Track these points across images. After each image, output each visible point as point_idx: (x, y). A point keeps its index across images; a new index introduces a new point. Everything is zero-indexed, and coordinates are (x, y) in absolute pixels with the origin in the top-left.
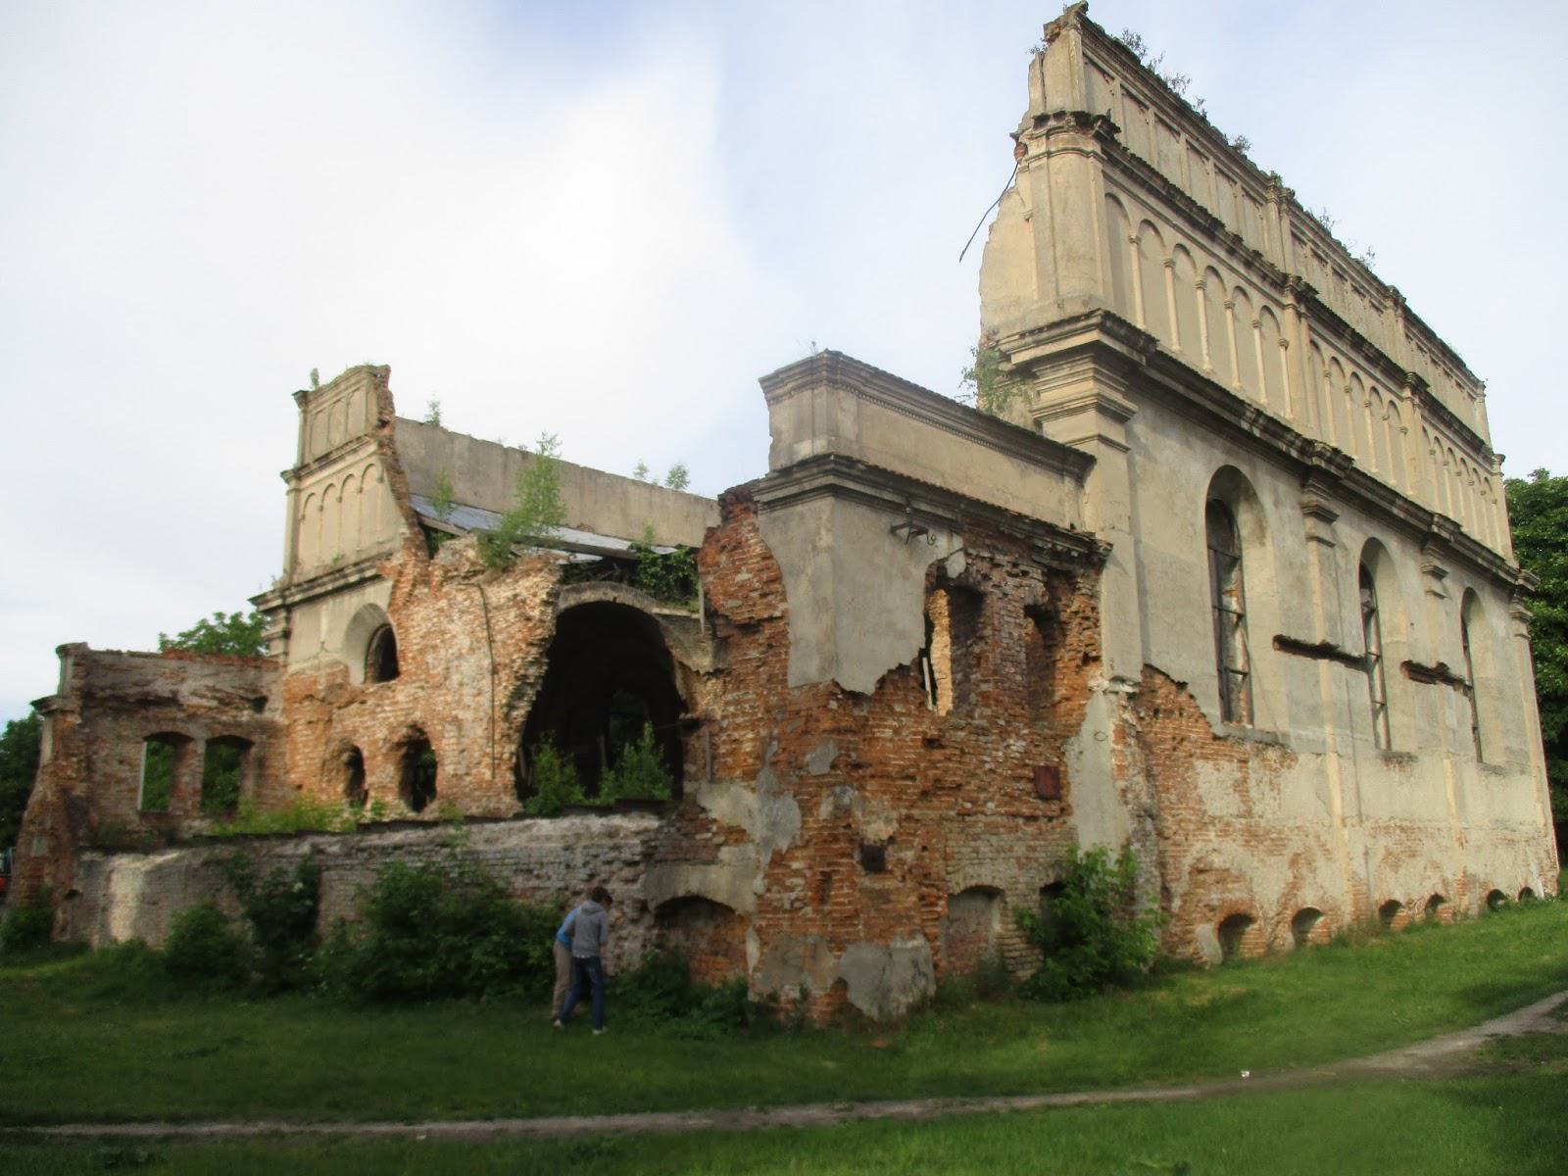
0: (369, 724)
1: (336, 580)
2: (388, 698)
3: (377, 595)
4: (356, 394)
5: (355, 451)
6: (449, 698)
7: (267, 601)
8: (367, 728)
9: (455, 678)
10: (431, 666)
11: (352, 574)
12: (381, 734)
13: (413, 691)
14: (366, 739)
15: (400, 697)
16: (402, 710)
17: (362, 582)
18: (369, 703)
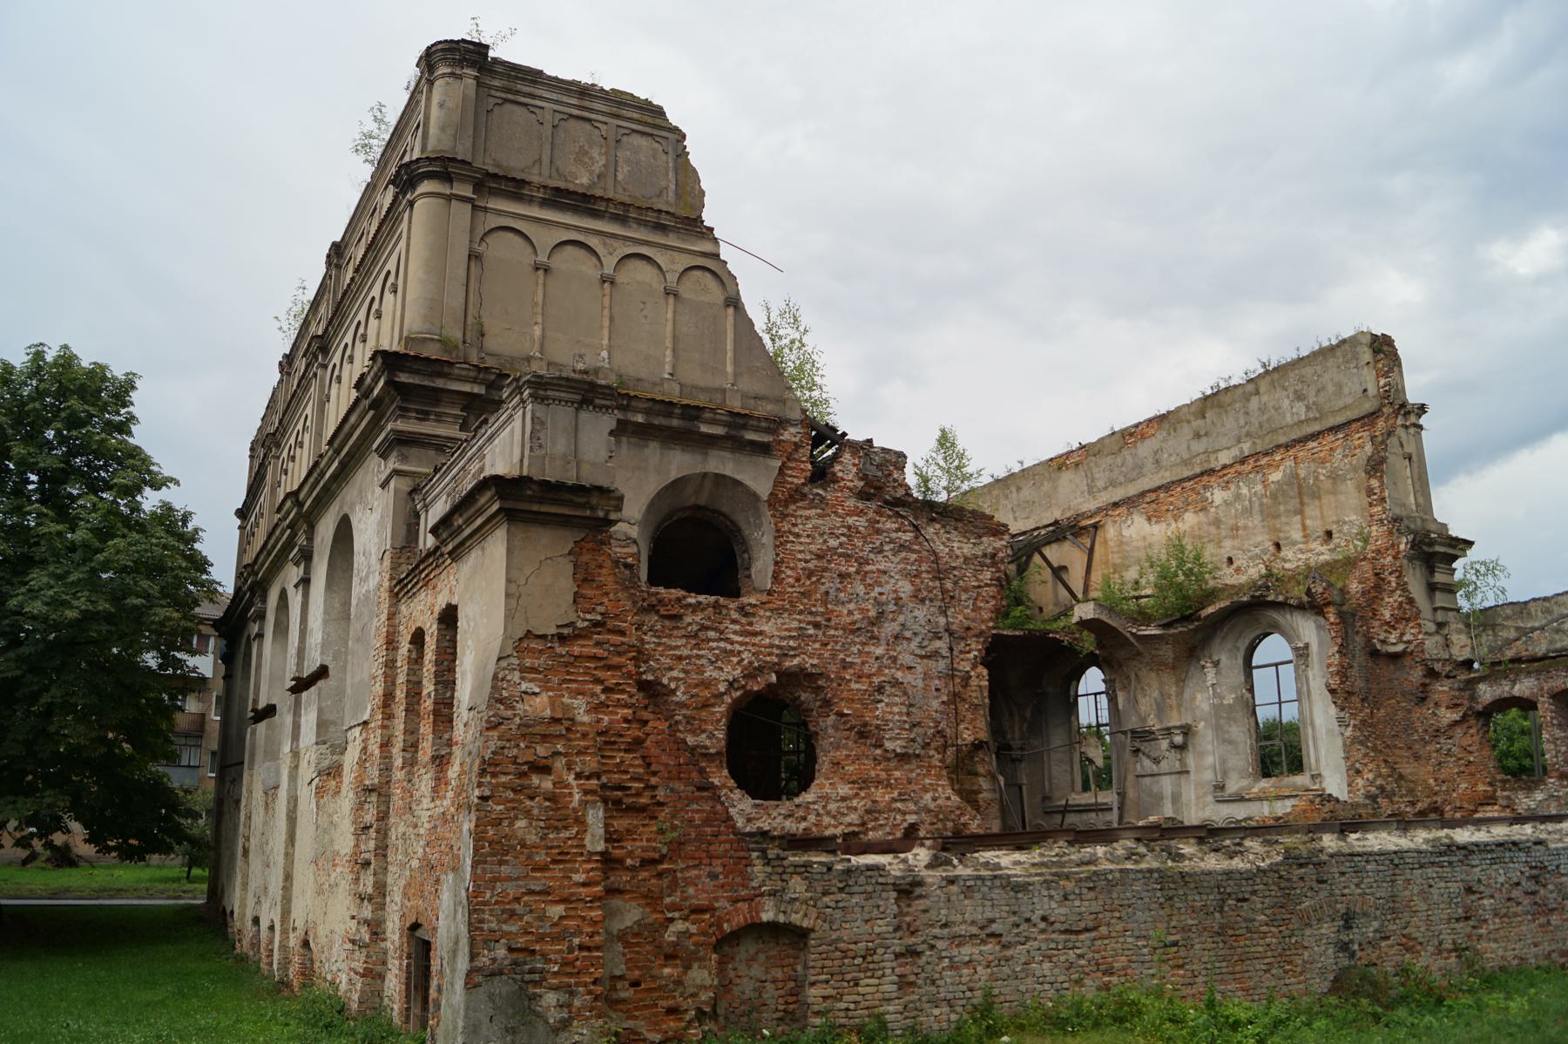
0: (686, 652)
1: (669, 415)
2: (734, 622)
3: (758, 478)
4: (637, 140)
5: (660, 228)
6: (879, 651)
7: (446, 376)
8: (680, 658)
9: (889, 628)
10: (831, 597)
11: (713, 422)
12: (731, 671)
13: (795, 624)
14: (675, 674)
15: (765, 628)
16: (772, 646)
17: (710, 442)
18: (688, 619)
